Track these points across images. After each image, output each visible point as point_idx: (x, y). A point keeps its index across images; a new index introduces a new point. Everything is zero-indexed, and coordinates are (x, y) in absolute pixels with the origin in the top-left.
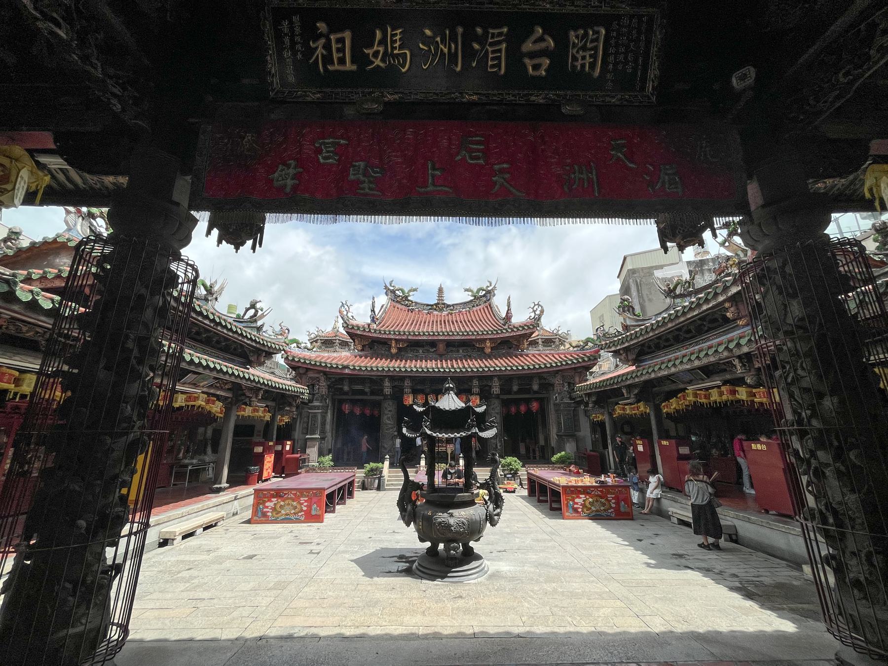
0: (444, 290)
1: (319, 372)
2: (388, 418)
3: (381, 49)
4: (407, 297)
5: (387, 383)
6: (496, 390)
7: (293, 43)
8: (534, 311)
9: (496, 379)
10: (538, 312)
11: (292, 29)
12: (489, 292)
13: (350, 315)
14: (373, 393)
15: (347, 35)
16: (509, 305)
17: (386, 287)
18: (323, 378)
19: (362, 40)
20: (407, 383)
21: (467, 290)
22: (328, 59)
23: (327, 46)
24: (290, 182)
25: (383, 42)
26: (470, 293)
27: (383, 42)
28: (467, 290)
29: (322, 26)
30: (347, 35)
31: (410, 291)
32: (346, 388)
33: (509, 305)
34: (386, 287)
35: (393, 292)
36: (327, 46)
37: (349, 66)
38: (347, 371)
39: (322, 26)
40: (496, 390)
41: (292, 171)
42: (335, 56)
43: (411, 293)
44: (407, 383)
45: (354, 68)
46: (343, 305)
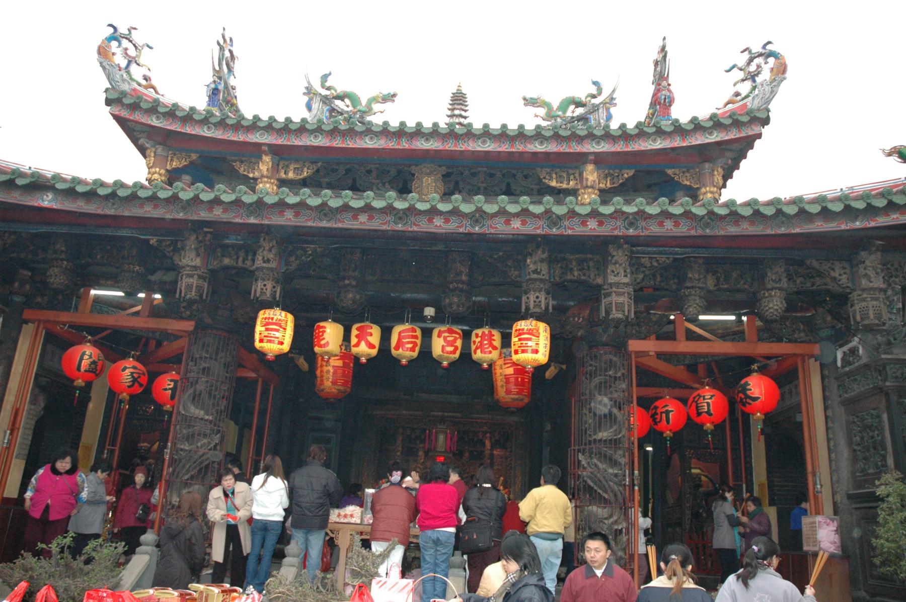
0: (470, 101)
2: (196, 398)
4: (364, 113)
6: (619, 302)
8: (752, 77)
9: (620, 256)
10: (765, 76)
12: (595, 109)
13: (137, 73)
16: (661, 78)
17: (309, 91)
20: (266, 259)
21: (530, 102)
26: (542, 111)
28: (530, 102)
31: (374, 100)
33: (661, 78)
34: (309, 91)
35: (325, 100)
38: (47, 201)
40: (619, 302)
43: (376, 107)
44: (266, 259)
46: (116, 36)
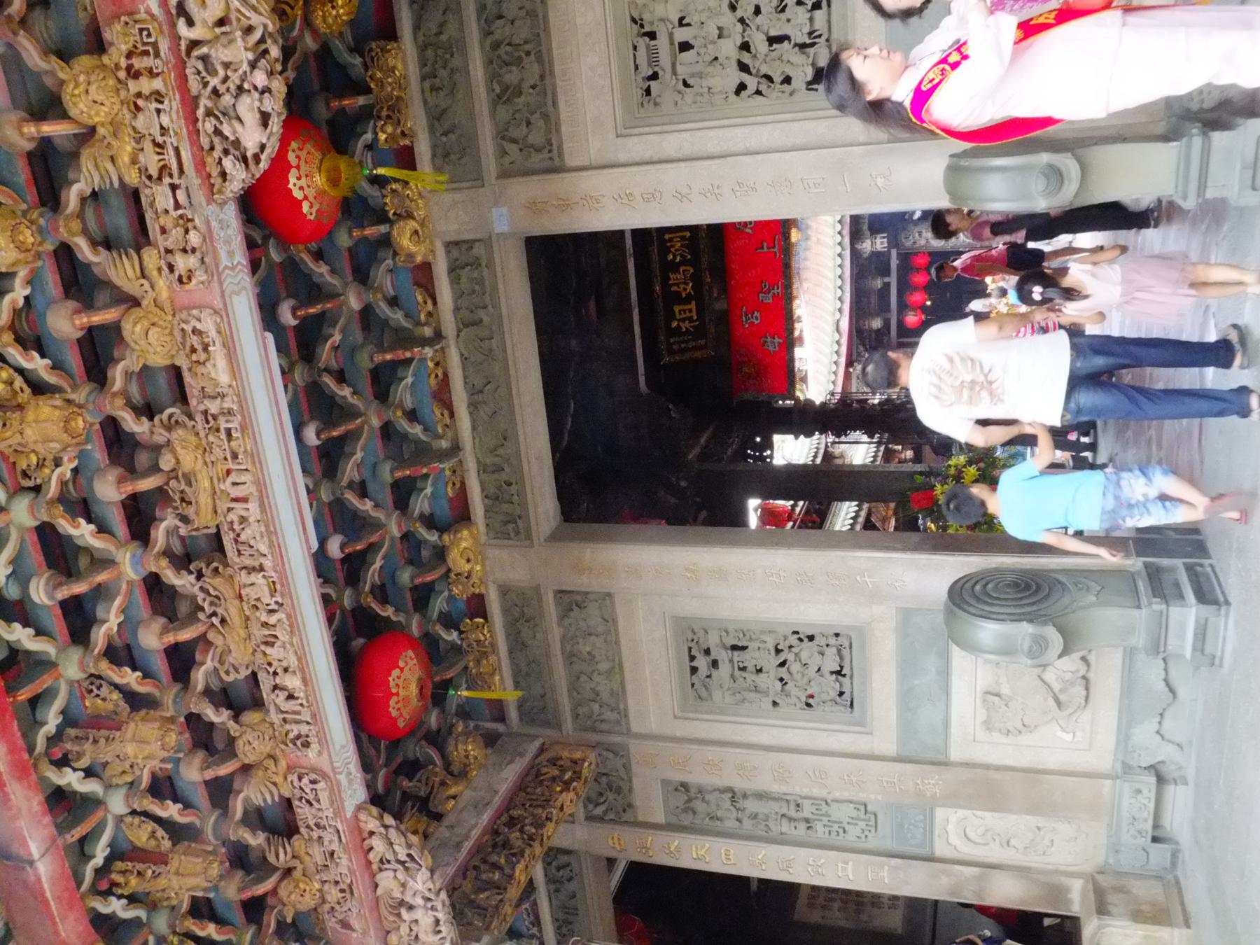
3: (682, 286)
5: (866, 246)
7: (683, 342)
11: (675, 343)
14: (886, 272)
15: (677, 309)
19: (678, 298)
22: (690, 319)
23: (683, 320)
24: (777, 340)
25: (677, 285)
27: (677, 285)
29: (675, 324)
30: (677, 309)
32: (877, 324)
36: (683, 320)
37: (693, 305)
39: (675, 324)
41: (769, 339)
42: (688, 314)
45: (694, 303)
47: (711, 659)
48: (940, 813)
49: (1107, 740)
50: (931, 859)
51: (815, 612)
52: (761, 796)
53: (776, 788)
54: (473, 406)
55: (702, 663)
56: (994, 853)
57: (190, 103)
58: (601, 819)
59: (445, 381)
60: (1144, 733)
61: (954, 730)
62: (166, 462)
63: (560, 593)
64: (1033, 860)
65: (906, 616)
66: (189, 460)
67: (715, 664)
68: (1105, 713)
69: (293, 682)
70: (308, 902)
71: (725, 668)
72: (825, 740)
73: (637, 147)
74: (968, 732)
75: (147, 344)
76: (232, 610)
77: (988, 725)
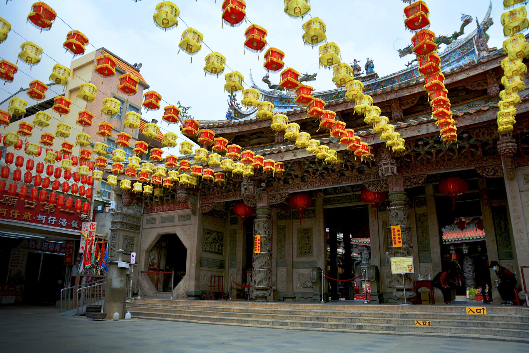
1: (364, 246)
18: (366, 249)
47: (306, 233)
48: (285, 268)
49: (298, 291)
50: (277, 267)
51: (315, 249)
52: (285, 241)
53: (286, 244)
54: (343, 197)
55: (305, 232)
56: (279, 276)
57: (374, 181)
58: (277, 215)
59: (347, 192)
60: (300, 295)
61: (298, 269)
62: (333, 174)
63: (315, 209)
64: (279, 282)
65: (315, 262)
66: (333, 177)
67: (305, 234)
68: (302, 290)
69: (306, 187)
70: (274, 185)
71: (305, 235)
72: (294, 250)
73: (380, 223)
74: (297, 272)
75: (347, 173)
76: (315, 180)
77: (299, 274)
